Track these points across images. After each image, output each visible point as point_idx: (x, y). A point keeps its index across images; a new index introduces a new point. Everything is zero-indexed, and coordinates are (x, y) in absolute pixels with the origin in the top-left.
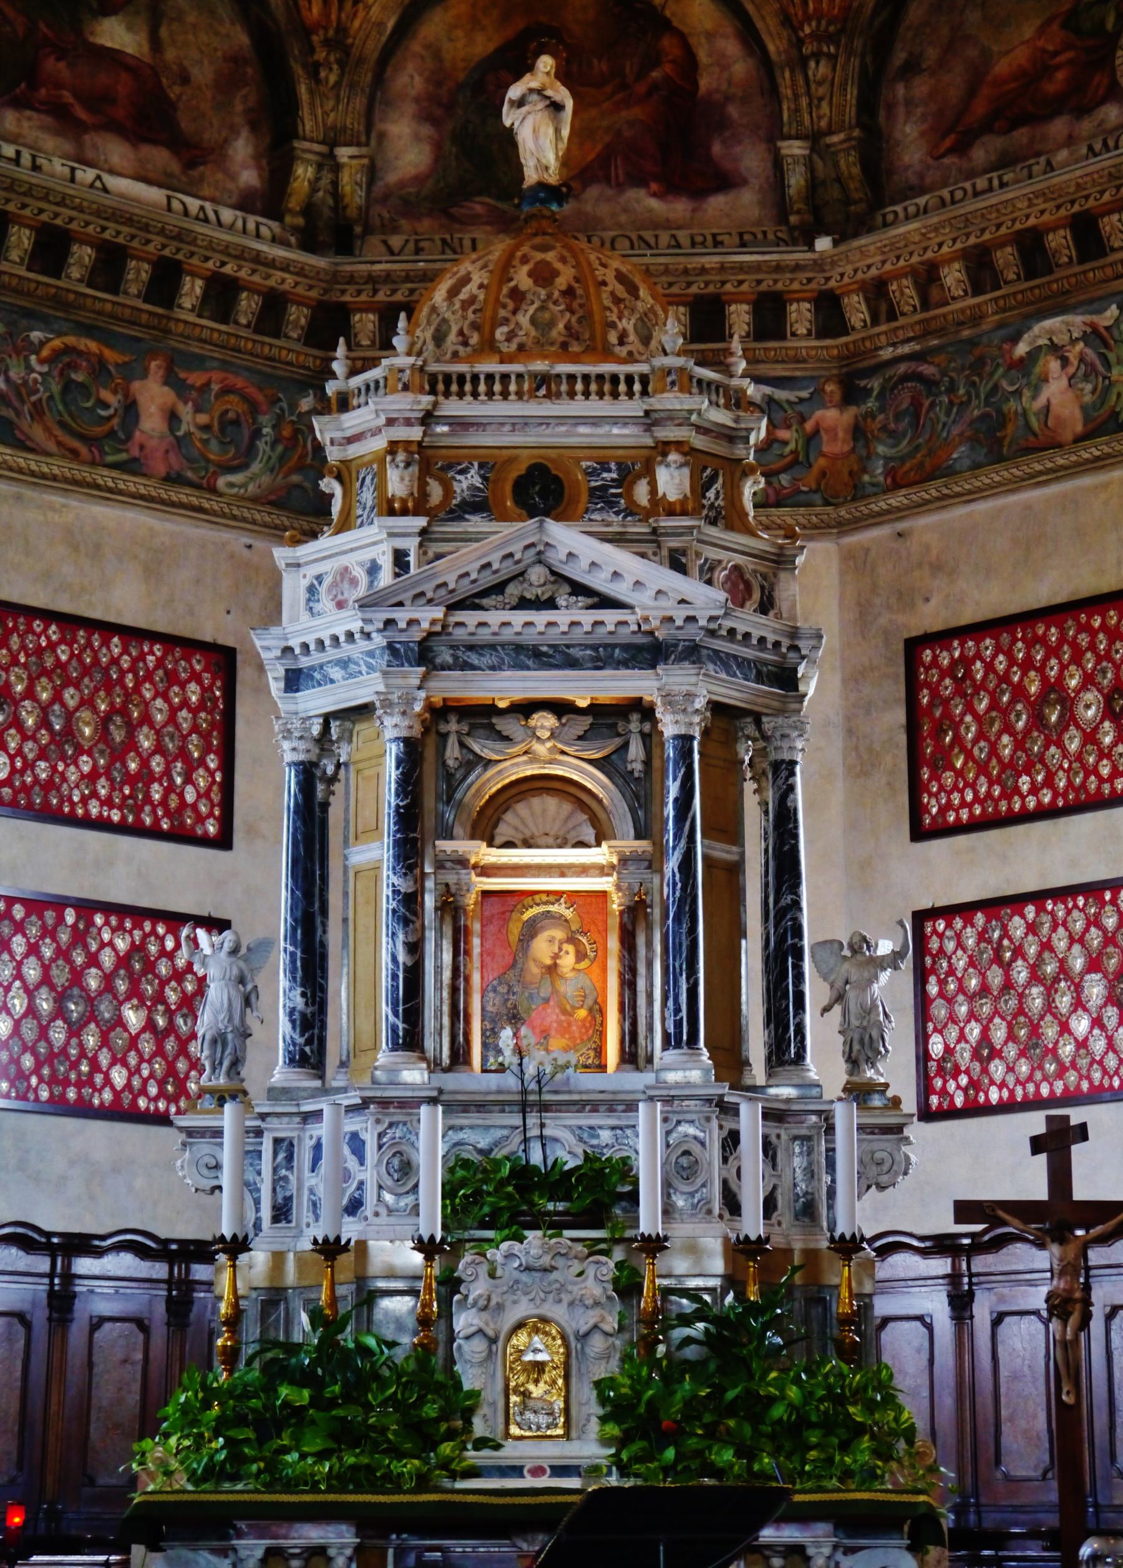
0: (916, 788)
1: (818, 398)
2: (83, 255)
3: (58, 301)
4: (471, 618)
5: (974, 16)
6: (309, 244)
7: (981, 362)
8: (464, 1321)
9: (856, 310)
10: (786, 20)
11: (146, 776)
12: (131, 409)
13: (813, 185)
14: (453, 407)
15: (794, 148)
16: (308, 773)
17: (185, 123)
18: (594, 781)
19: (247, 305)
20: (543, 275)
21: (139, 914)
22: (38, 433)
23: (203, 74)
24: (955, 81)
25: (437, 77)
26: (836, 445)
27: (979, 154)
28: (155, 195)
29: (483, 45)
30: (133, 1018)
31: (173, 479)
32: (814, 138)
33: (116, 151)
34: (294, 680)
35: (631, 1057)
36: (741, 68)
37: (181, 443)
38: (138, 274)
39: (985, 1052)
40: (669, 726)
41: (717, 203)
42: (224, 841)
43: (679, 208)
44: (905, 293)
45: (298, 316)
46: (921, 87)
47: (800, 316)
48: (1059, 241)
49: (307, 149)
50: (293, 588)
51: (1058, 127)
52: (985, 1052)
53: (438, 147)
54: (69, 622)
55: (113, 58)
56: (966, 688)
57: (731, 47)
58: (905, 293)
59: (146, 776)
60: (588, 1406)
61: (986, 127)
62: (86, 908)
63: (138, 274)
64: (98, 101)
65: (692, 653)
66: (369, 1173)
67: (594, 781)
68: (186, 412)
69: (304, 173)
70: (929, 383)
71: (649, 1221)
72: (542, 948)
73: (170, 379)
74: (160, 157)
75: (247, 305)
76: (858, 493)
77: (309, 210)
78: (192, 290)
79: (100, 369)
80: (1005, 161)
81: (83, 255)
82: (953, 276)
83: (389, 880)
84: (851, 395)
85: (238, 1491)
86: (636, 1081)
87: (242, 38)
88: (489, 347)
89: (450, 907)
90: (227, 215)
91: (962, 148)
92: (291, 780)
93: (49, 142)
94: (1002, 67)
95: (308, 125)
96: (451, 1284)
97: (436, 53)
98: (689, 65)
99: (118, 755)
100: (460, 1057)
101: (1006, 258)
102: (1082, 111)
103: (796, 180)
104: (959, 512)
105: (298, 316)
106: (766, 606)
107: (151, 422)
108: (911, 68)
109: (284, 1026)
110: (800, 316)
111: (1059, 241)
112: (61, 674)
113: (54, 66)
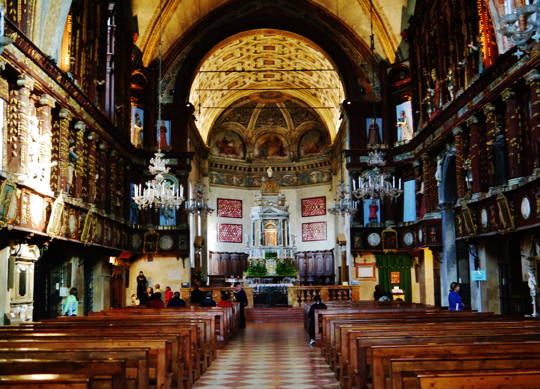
0: (302, 213)
1: (294, 176)
2: (229, 167)
3: (227, 171)
4: (265, 214)
5: (308, 142)
6: (247, 162)
7: (308, 175)
8: (266, 265)
9: (297, 169)
10: (291, 141)
11: (235, 213)
12: (233, 180)
13: (294, 156)
14: (264, 197)
15: (292, 153)
16: (254, 224)
17: (237, 152)
18: (274, 224)
19: (243, 169)
20: (270, 186)
21: (235, 225)
22: (225, 183)
23: (238, 147)
24: (306, 148)
25: (259, 145)
26: (295, 181)
27: (308, 155)
28: (234, 160)
29: (263, 142)
30: (234, 234)
31: (236, 186)
32: (293, 152)
33: (231, 156)
34: (253, 217)
35: (277, 244)
36: (287, 144)
37: (237, 182)
38: (233, 168)
39: (308, 236)
40: (280, 221)
41: (285, 157)
42: (241, 218)
43: (281, 158)
44: (301, 168)
45: (247, 169)
46: (303, 148)
47: (292, 169)
48: (314, 165)
49: (247, 153)
50: (252, 210)
51: (315, 154)
52: (308, 236)
53: (259, 153)
54: (228, 200)
55: (230, 147)
56: (307, 204)
57: (286, 142)
58: (301, 168)
59: (235, 213)
60: (275, 270)
61: (308, 153)
62: (231, 224)
63: (233, 168)
64: (229, 151)
65: (282, 216)
66: (259, 253)
67: (274, 224)
68: (238, 180)
69: (247, 156)
70: (304, 176)
71: (278, 257)
72: (271, 236)
73: (236, 177)
74: (234, 156)
75: (243, 169)
76: (297, 185)
77: (248, 159)
78: (238, 168)
79: (230, 176)
80: (310, 156)
81: (229, 167)
82: (305, 167)
83: (260, 233)
84: (297, 176)
85: (252, 275)
86: (278, 247)
87: (241, 143)
88: (266, 192)
89: (264, 234)
90: (241, 160)
91: (307, 154)
92: (252, 224)
93: (226, 156)
94: (310, 147)
95: (248, 151)
96: (265, 262)
97: (259, 143)
98: (282, 144)
99: (233, 211)
100: (265, 245)
101: (310, 166)
102: (317, 153)
103: (292, 156)
104: (306, 188)
105: (247, 169)
106: (287, 211)
107: (234, 181)
108: (302, 146)
109: (252, 243)
110: (292, 169)
111: (314, 165)
112: (228, 204)
113: (226, 149)
